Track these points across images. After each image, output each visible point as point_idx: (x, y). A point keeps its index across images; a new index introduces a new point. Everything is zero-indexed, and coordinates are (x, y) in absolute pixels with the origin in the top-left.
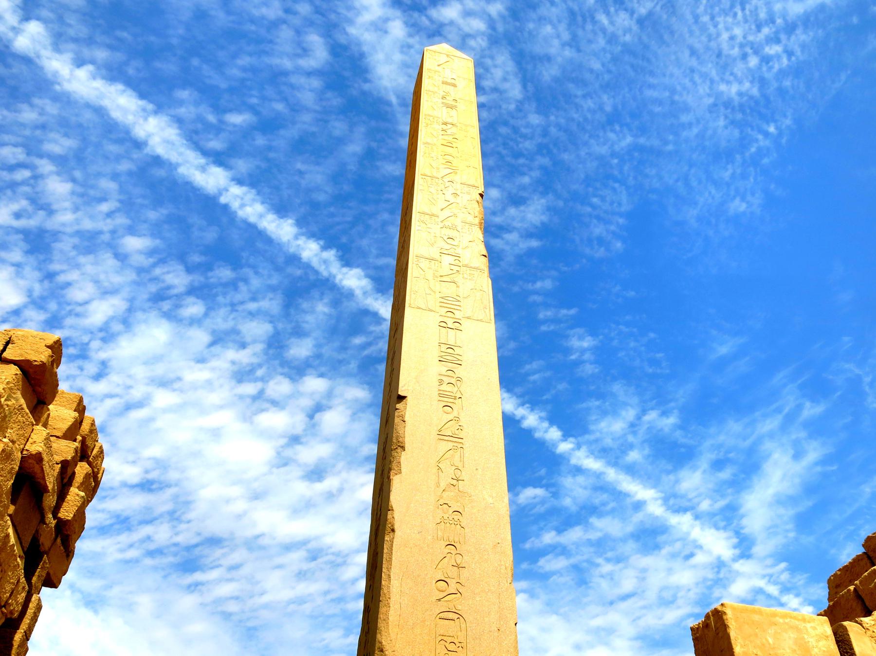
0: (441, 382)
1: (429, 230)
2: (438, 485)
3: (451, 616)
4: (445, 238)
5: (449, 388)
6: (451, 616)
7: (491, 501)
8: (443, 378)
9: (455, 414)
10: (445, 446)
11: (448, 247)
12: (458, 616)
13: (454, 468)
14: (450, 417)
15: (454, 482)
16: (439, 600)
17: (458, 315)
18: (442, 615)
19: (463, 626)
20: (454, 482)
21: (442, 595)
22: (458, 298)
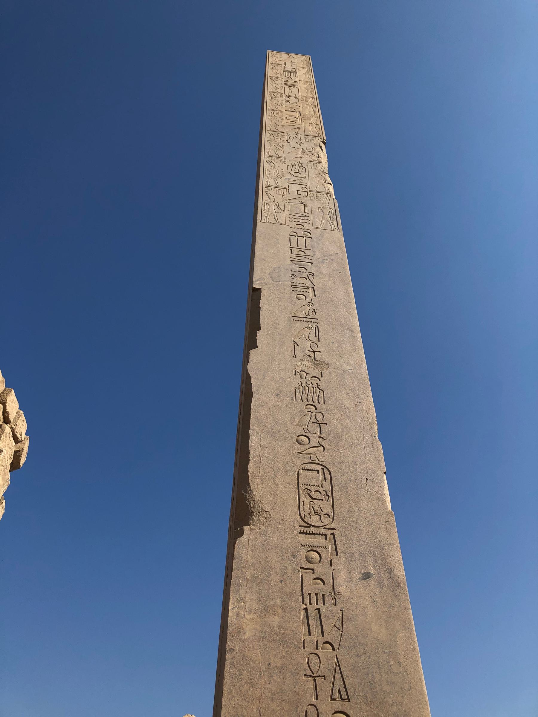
0: (294, 276)
1: (276, 167)
2: (295, 356)
3: (314, 466)
4: (293, 173)
5: (303, 281)
6: (314, 466)
7: (348, 367)
8: (296, 274)
9: (308, 300)
10: (298, 325)
11: (294, 178)
12: (321, 467)
13: (309, 342)
14: (305, 302)
15: (312, 354)
16: (301, 453)
17: (307, 226)
18: (305, 466)
19: (328, 476)
20: (312, 354)
21: (302, 448)
22: (307, 214)
